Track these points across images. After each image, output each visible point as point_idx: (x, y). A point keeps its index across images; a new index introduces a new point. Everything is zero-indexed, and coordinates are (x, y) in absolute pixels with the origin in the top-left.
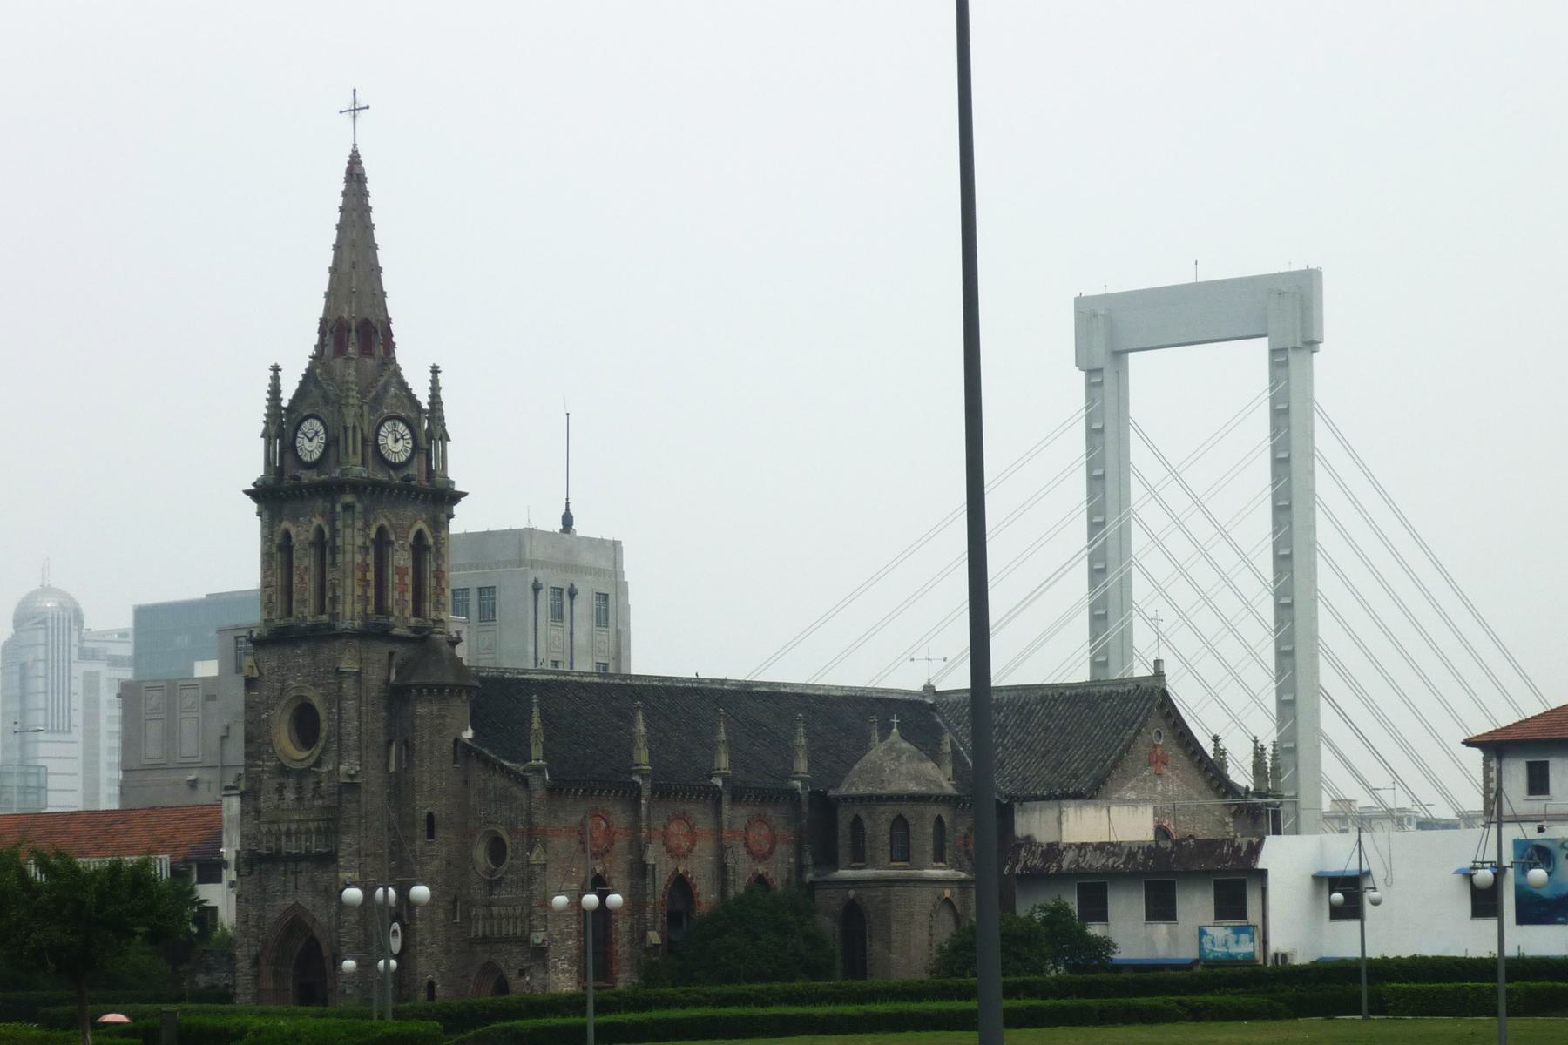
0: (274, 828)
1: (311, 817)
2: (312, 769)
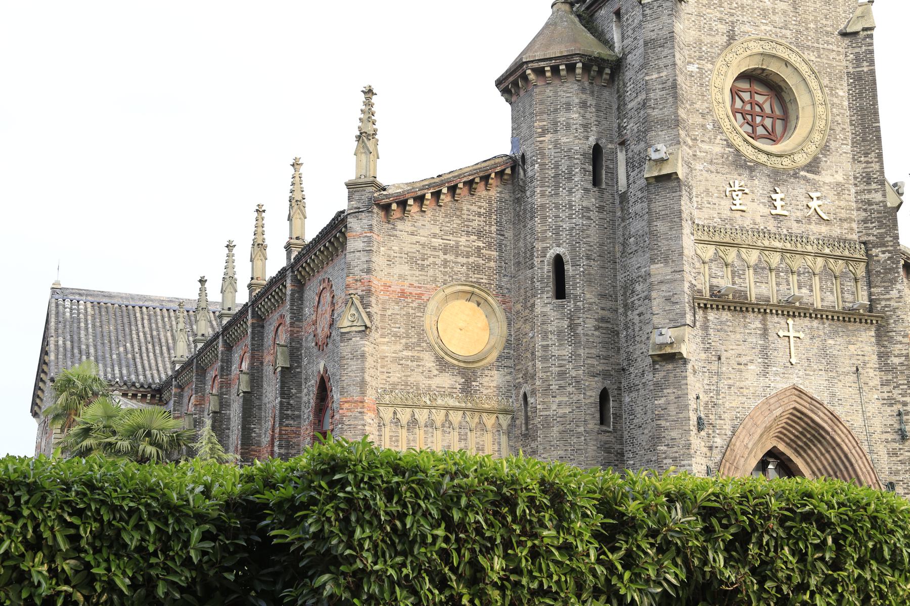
0: (731, 255)
1: (809, 248)
2: (802, 173)
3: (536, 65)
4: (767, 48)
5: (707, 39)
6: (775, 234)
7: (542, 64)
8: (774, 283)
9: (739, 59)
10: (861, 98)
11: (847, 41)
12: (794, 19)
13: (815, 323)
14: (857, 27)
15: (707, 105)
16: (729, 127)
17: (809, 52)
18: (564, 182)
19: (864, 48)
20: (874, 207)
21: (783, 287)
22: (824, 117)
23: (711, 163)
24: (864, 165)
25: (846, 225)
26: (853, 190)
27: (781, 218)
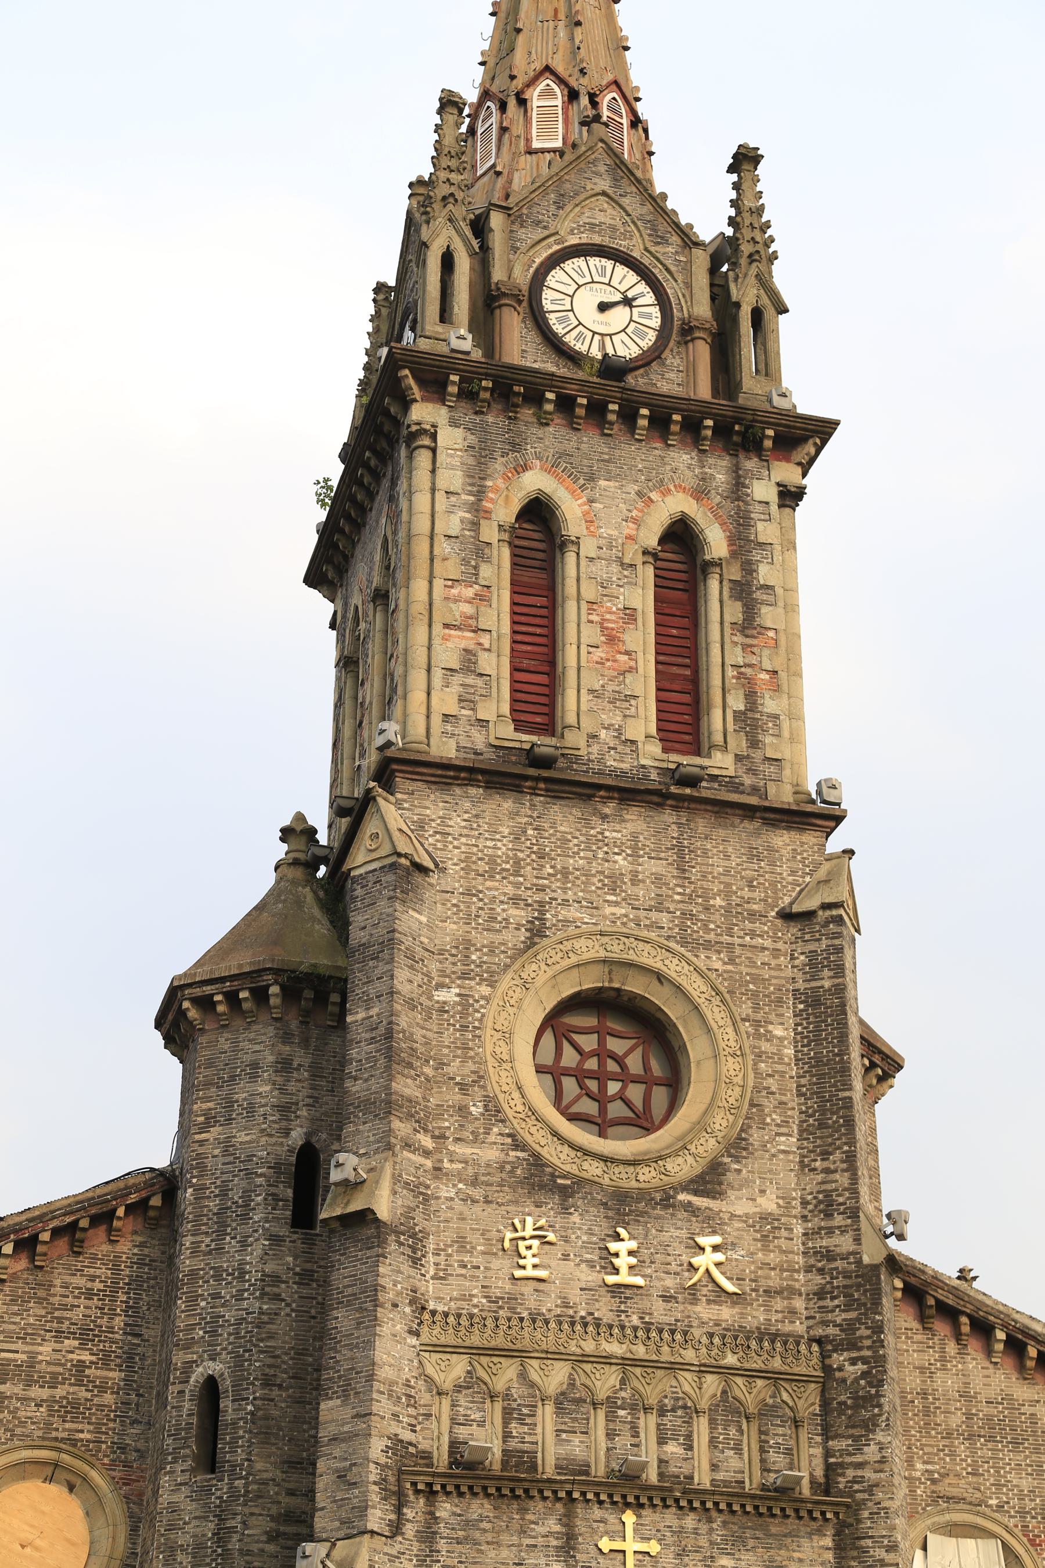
1: (689, 1355)
2: (682, 1197)
3: (197, 992)
4: (616, 948)
5: (481, 939)
6: (611, 1326)
7: (208, 989)
8: (601, 1433)
9: (550, 973)
10: (818, 1041)
11: (794, 929)
12: (680, 890)
13: (690, 1521)
14: (811, 903)
15: (473, 1068)
16: (520, 1108)
17: (709, 953)
18: (234, 1225)
19: (824, 943)
20: (839, 1264)
21: (623, 1441)
22: (738, 1080)
23: (474, 1182)
24: (820, 1177)
25: (779, 1304)
26: (799, 1230)
27: (628, 1293)
